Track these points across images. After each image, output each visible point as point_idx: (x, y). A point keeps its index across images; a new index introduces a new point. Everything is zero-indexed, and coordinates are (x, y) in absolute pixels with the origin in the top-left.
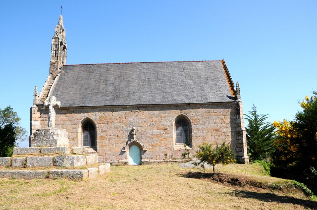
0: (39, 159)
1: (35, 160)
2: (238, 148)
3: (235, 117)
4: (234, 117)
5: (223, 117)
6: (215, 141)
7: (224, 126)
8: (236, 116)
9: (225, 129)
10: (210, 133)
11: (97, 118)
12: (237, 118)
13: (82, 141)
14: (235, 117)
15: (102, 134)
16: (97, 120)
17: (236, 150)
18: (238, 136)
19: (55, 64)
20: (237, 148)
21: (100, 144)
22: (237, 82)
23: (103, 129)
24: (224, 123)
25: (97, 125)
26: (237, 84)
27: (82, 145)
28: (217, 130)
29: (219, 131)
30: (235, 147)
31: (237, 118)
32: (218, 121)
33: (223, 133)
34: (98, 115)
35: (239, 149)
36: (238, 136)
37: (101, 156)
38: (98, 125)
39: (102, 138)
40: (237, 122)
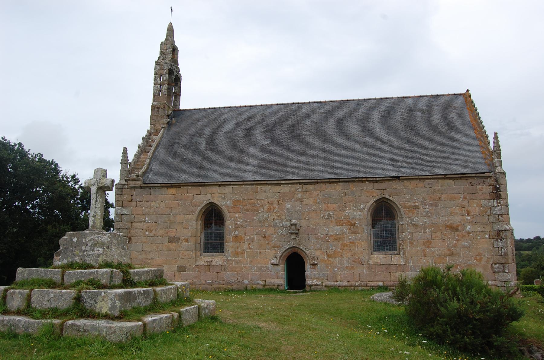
0: (52, 295)
1: (47, 296)
2: (498, 265)
3: (490, 204)
4: (489, 202)
5: (465, 203)
6: (449, 250)
7: (467, 219)
8: (492, 200)
9: (469, 227)
10: (439, 234)
11: (228, 203)
12: (496, 205)
13: (202, 243)
14: (490, 204)
15: (237, 232)
16: (228, 206)
17: (492, 267)
18: (497, 240)
19: (159, 108)
20: (495, 264)
21: (233, 250)
22: (496, 134)
23: (238, 223)
24: (468, 214)
25: (227, 215)
26: (496, 137)
27: (203, 251)
28: (453, 229)
29: (457, 230)
30: (491, 263)
31: (496, 205)
32: (457, 210)
33: (467, 235)
34: (230, 198)
35: (498, 267)
36: (497, 240)
37: (235, 271)
38: (230, 216)
39: (237, 239)
40: (494, 213)
